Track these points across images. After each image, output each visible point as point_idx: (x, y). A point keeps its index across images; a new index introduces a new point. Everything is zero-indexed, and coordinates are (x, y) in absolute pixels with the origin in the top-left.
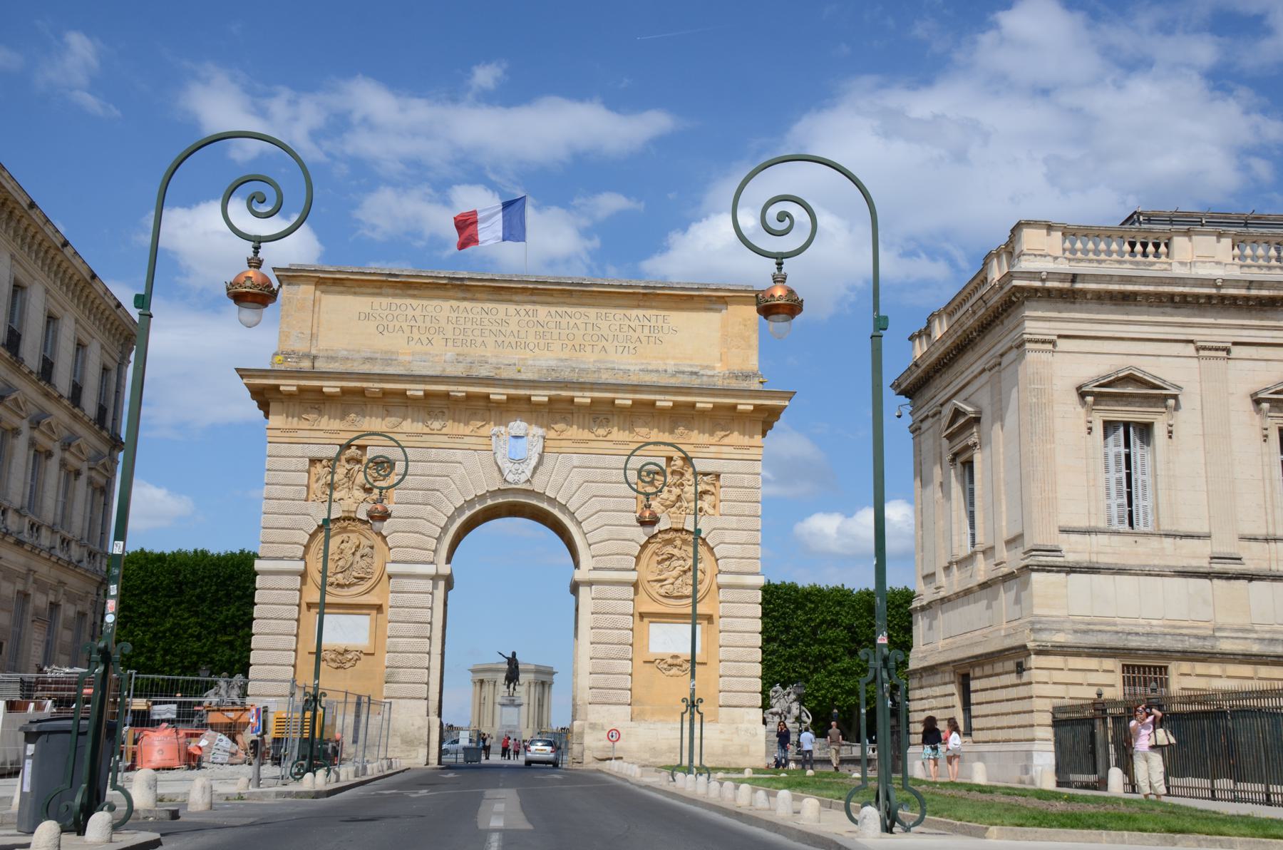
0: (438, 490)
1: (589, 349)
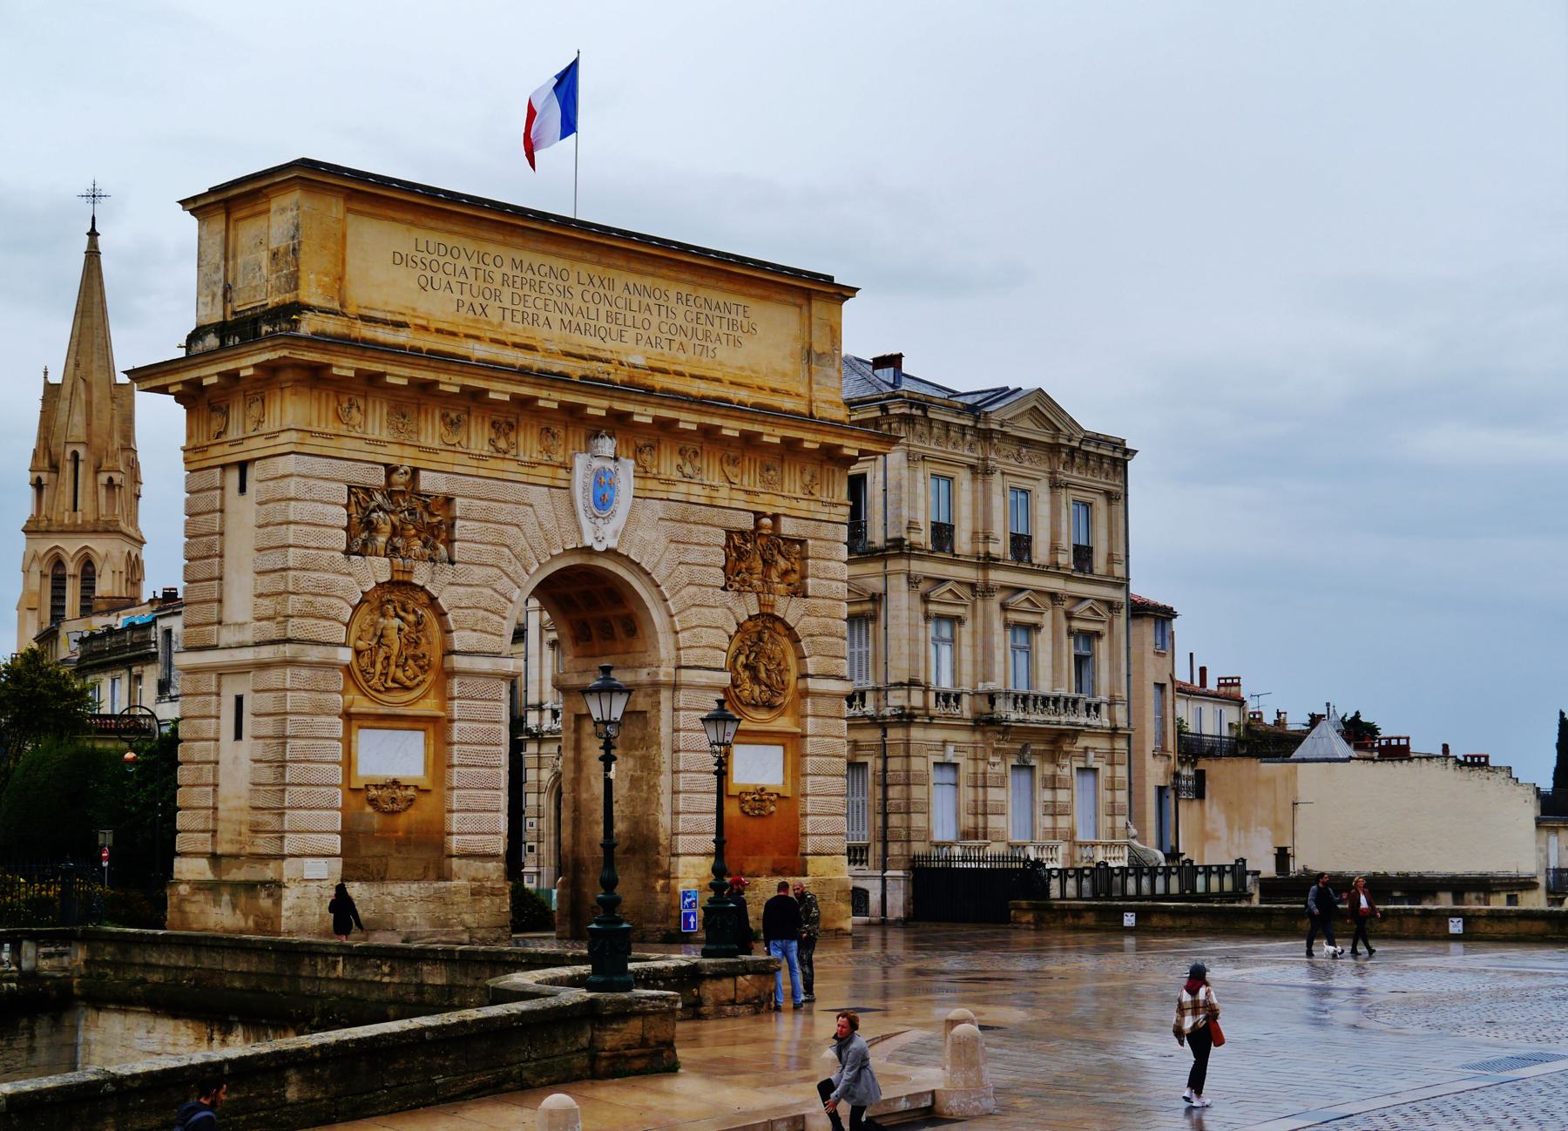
0: (506, 546)
1: (665, 344)
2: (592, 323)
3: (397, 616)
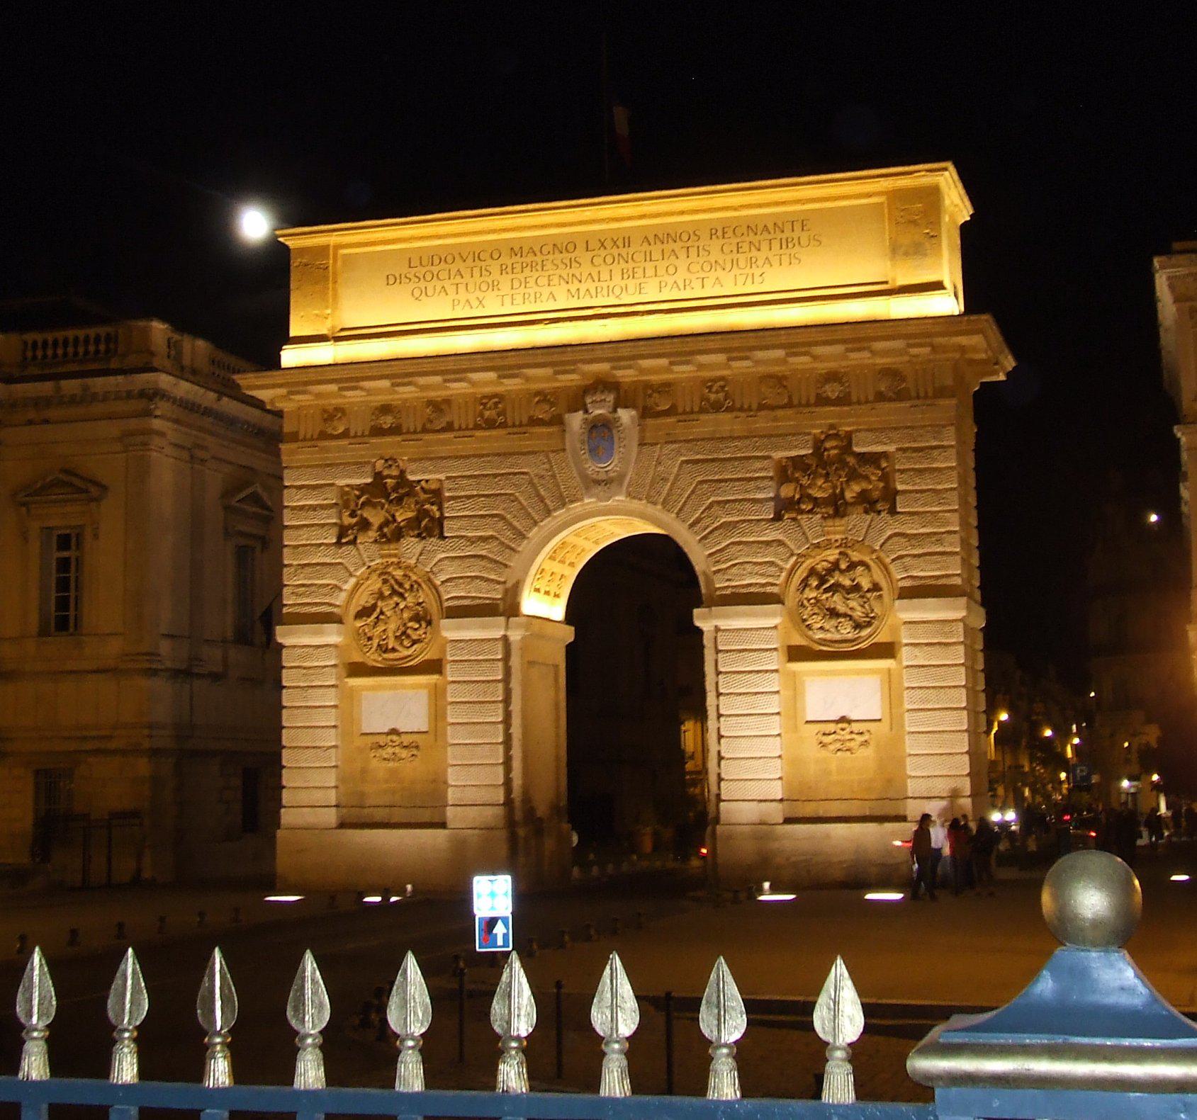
2: (604, 285)
3: (394, 592)
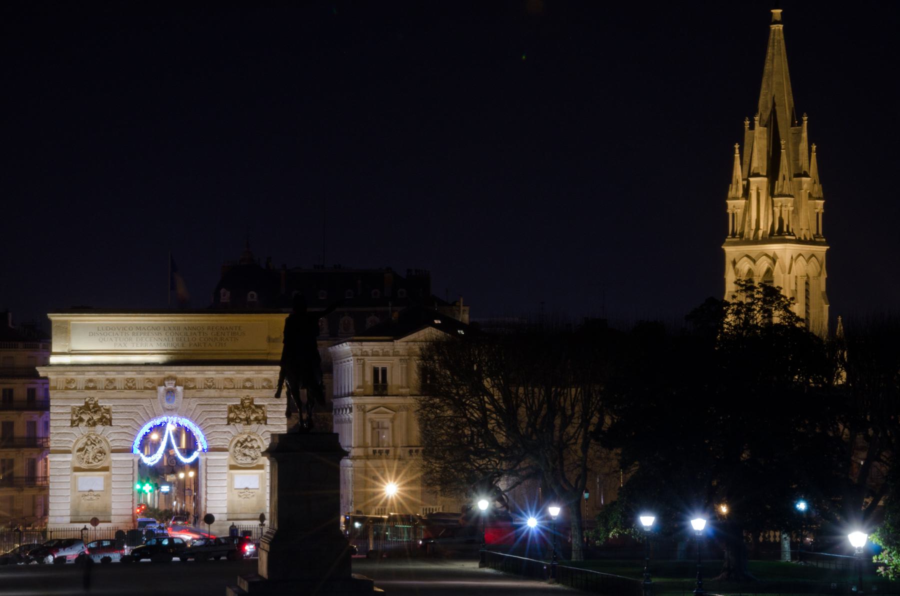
3: (92, 443)
